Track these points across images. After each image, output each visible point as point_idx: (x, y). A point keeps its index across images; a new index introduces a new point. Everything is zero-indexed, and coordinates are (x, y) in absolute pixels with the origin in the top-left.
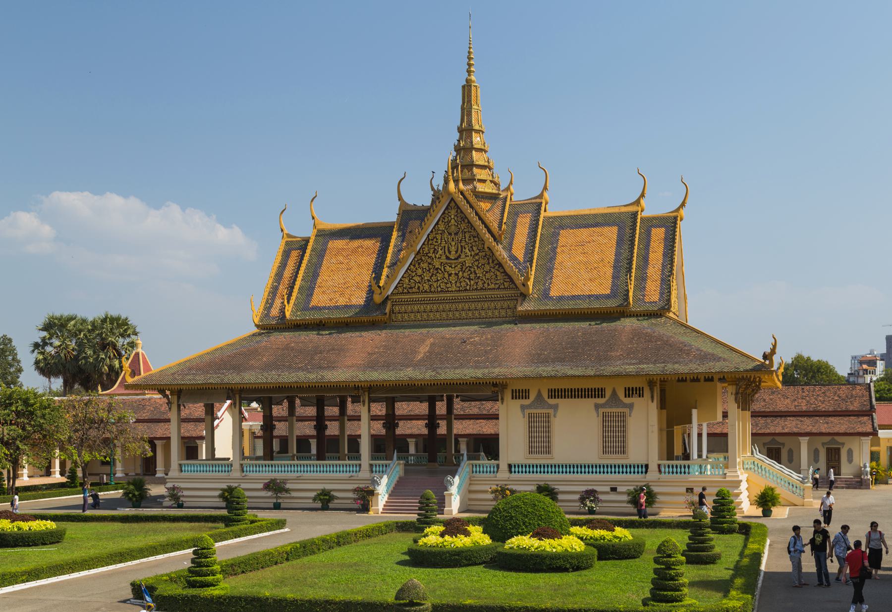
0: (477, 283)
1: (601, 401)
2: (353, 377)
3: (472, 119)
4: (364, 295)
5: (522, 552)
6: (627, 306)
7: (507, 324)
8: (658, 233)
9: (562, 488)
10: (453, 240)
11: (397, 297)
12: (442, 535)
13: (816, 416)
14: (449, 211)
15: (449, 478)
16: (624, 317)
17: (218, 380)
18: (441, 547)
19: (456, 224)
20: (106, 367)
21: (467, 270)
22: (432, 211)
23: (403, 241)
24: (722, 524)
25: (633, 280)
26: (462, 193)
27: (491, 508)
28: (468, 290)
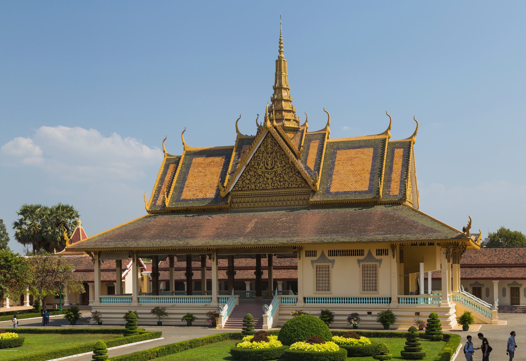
0: (284, 184)
1: (361, 258)
2: (206, 243)
3: (282, 81)
4: (215, 192)
5: (300, 352)
6: (378, 198)
7: (303, 209)
8: (399, 152)
9: (336, 312)
10: (269, 157)
11: (235, 193)
12: (252, 341)
13: (504, 267)
14: (267, 139)
15: (265, 306)
16: (376, 205)
17: (123, 246)
18: (250, 348)
19: (272, 147)
20: (59, 237)
21: (278, 176)
22: (256, 139)
23: (239, 158)
24: (433, 335)
25: (383, 182)
26: (275, 128)
27: (282, 325)
28: (279, 189)
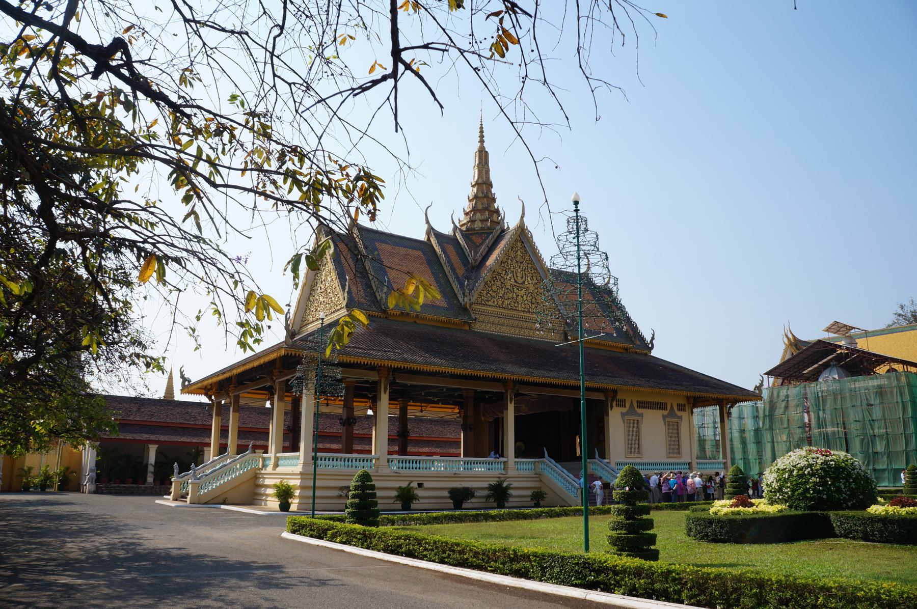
1: (666, 412)
21: (529, 295)
